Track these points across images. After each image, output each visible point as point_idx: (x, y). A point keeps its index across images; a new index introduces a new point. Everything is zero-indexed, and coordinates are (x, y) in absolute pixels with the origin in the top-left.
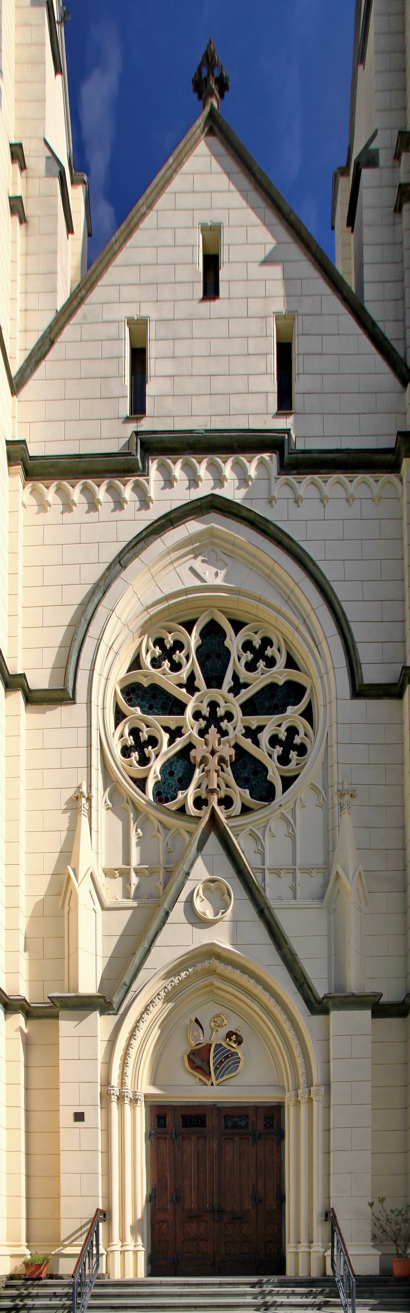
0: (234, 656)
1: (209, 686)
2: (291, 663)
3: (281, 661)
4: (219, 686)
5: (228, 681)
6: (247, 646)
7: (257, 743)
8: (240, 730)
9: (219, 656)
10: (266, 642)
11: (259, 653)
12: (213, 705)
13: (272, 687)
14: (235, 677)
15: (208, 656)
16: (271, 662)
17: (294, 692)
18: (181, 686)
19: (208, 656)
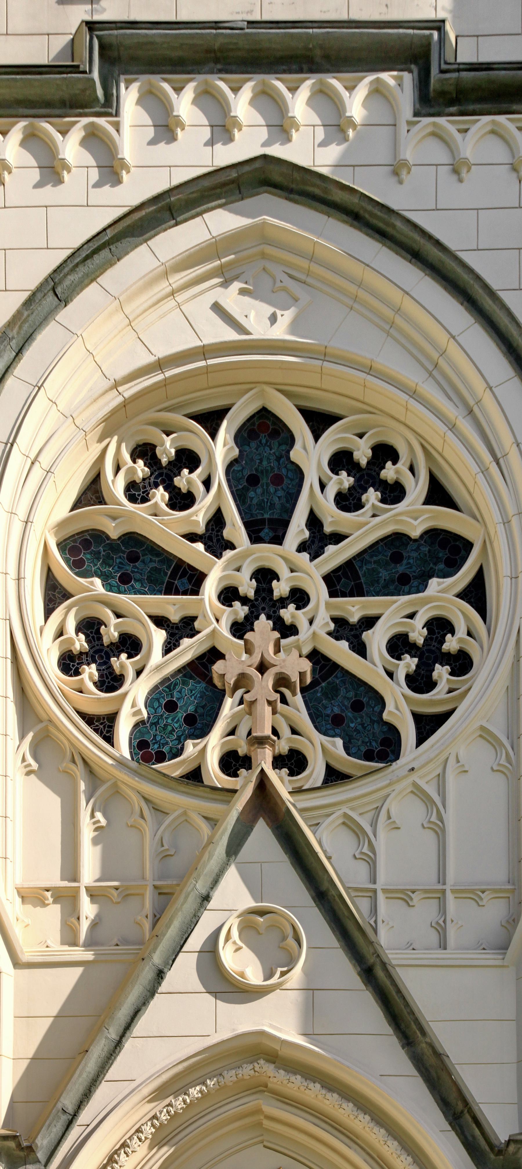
0: (311, 479)
1: (255, 538)
2: (438, 494)
3: (416, 489)
4: (278, 540)
5: (297, 529)
6: (341, 461)
7: (360, 649)
8: (324, 622)
9: (278, 480)
10: (384, 453)
11: (367, 475)
12: (265, 576)
13: (396, 541)
14: (314, 521)
15: (253, 480)
16: (394, 493)
17: (447, 550)
18: (192, 537)
19: (253, 480)
